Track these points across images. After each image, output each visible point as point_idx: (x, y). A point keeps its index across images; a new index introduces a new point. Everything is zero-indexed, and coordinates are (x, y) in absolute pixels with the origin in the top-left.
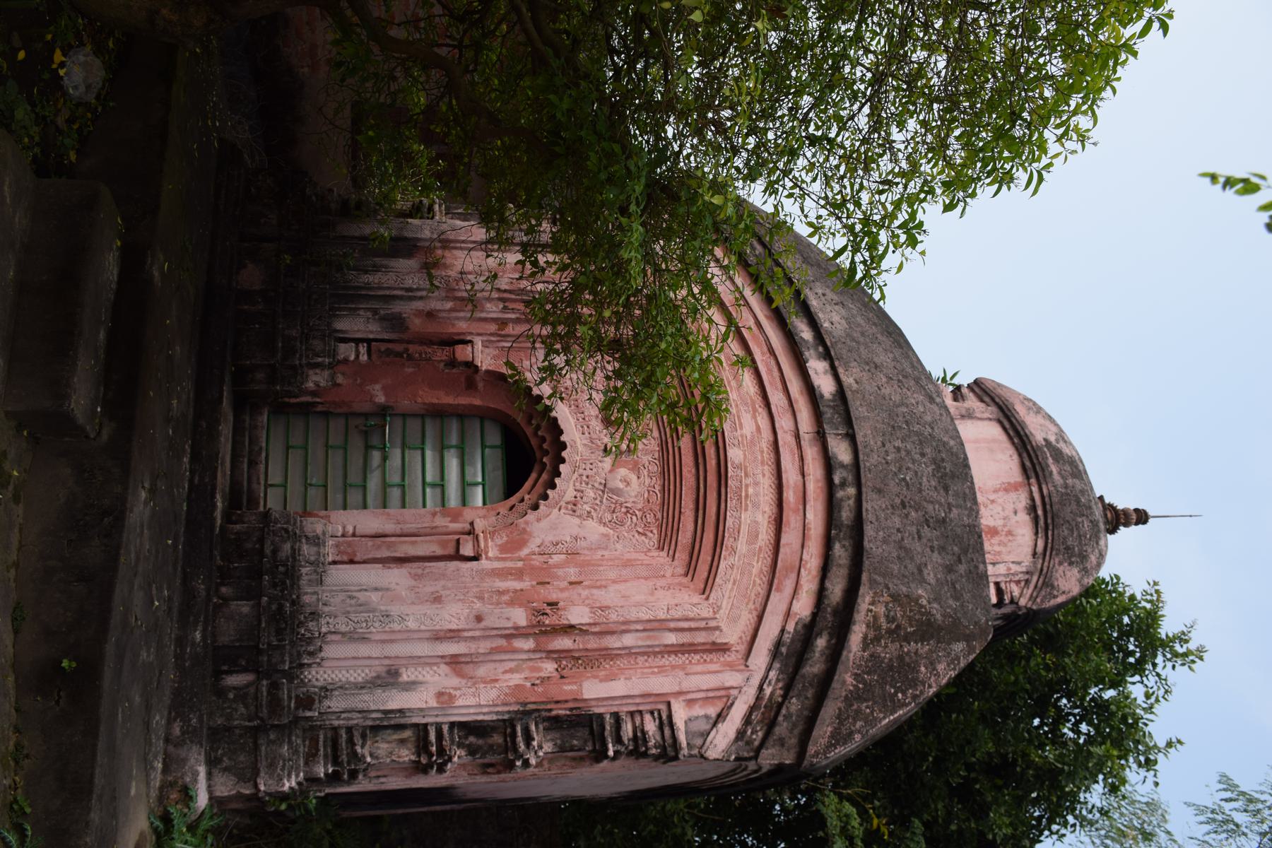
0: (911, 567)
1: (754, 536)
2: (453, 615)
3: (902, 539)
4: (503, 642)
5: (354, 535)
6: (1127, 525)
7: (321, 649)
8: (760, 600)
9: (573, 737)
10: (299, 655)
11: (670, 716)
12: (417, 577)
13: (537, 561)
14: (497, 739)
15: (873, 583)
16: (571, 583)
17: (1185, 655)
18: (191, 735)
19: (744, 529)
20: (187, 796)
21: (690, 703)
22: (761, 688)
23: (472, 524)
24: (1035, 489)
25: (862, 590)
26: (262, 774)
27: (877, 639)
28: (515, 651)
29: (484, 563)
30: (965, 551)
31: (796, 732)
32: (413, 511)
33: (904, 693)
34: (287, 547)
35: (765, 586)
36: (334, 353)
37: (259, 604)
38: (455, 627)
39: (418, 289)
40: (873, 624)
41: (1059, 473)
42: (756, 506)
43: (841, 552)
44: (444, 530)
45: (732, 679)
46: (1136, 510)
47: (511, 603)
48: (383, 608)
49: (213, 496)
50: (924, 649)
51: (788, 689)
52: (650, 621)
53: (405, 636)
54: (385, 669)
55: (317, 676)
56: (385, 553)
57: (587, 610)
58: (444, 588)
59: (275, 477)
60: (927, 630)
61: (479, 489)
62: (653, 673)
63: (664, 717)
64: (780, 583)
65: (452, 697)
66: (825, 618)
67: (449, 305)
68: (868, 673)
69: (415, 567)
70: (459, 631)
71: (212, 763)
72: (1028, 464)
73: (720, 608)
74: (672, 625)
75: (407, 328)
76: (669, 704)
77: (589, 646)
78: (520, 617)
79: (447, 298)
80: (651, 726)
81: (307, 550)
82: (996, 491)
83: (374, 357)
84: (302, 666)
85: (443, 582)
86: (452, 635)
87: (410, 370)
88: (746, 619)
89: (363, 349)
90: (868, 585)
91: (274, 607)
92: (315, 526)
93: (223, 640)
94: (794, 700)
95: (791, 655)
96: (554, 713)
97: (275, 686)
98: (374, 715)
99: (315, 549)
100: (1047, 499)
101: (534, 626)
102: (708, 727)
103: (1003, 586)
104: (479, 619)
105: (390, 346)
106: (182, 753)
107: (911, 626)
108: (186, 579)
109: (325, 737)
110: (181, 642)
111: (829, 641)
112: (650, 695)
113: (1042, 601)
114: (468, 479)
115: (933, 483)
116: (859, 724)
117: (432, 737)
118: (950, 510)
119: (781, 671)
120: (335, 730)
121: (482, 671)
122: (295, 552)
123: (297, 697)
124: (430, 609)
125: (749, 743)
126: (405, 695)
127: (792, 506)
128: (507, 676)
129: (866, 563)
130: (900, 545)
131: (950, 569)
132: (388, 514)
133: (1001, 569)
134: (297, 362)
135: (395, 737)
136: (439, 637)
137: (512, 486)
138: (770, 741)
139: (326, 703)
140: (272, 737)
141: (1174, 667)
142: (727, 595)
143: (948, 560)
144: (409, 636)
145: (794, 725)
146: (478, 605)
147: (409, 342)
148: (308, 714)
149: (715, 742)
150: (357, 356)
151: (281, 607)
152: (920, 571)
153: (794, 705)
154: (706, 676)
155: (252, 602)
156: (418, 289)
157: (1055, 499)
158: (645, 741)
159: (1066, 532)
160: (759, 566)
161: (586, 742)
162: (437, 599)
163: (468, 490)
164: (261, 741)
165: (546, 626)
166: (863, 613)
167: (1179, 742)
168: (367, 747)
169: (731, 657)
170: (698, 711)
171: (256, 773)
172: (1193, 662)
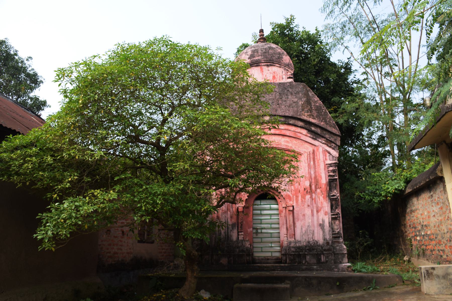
0: (294, 104)
2: (308, 212)
4: (313, 201)
5: (287, 235)
6: (263, 35)
8: (302, 141)
9: (333, 186)
10: (318, 245)
11: (329, 164)
12: (298, 220)
13: (293, 192)
14: (334, 202)
15: (300, 115)
17: (291, 19)
18: (336, 267)
19: (286, 144)
20: (349, 267)
21: (326, 159)
22: (323, 143)
24: (262, 64)
25: (302, 118)
27: (313, 116)
28: (315, 198)
29: (294, 205)
30: (286, 89)
31: (333, 136)
33: (323, 110)
34: (292, 249)
36: (242, 241)
40: (310, 116)
41: (258, 57)
42: (280, 140)
43: (292, 122)
45: (321, 150)
46: (260, 32)
47: (305, 199)
51: (323, 137)
55: (321, 241)
56: (292, 227)
57: (306, 182)
59: (269, 254)
60: (308, 102)
65: (326, 212)
67: (229, 213)
69: (296, 220)
71: (341, 263)
72: (255, 65)
78: (308, 197)
79: (227, 213)
80: (331, 169)
81: (292, 245)
82: (263, 75)
86: (312, 211)
88: (307, 145)
89: (240, 234)
92: (285, 244)
93: (315, 261)
95: (316, 136)
97: (325, 250)
104: (309, 206)
105: (239, 227)
106: (340, 268)
108: (303, 270)
110: (317, 270)
114: (269, 208)
117: (334, 216)
120: (333, 237)
121: (320, 205)
124: (306, 217)
125: (335, 147)
129: (295, 116)
130: (289, 107)
131: (292, 94)
133: (284, 77)
136: (313, 215)
139: (328, 239)
143: (289, 94)
144: (312, 221)
147: (238, 223)
151: (308, 249)
152: (294, 102)
153: (327, 136)
154: (320, 156)
157: (266, 59)
158: (334, 170)
160: (294, 141)
162: (304, 215)
165: (310, 191)
169: (315, 150)
170: (328, 158)
171: (343, 254)
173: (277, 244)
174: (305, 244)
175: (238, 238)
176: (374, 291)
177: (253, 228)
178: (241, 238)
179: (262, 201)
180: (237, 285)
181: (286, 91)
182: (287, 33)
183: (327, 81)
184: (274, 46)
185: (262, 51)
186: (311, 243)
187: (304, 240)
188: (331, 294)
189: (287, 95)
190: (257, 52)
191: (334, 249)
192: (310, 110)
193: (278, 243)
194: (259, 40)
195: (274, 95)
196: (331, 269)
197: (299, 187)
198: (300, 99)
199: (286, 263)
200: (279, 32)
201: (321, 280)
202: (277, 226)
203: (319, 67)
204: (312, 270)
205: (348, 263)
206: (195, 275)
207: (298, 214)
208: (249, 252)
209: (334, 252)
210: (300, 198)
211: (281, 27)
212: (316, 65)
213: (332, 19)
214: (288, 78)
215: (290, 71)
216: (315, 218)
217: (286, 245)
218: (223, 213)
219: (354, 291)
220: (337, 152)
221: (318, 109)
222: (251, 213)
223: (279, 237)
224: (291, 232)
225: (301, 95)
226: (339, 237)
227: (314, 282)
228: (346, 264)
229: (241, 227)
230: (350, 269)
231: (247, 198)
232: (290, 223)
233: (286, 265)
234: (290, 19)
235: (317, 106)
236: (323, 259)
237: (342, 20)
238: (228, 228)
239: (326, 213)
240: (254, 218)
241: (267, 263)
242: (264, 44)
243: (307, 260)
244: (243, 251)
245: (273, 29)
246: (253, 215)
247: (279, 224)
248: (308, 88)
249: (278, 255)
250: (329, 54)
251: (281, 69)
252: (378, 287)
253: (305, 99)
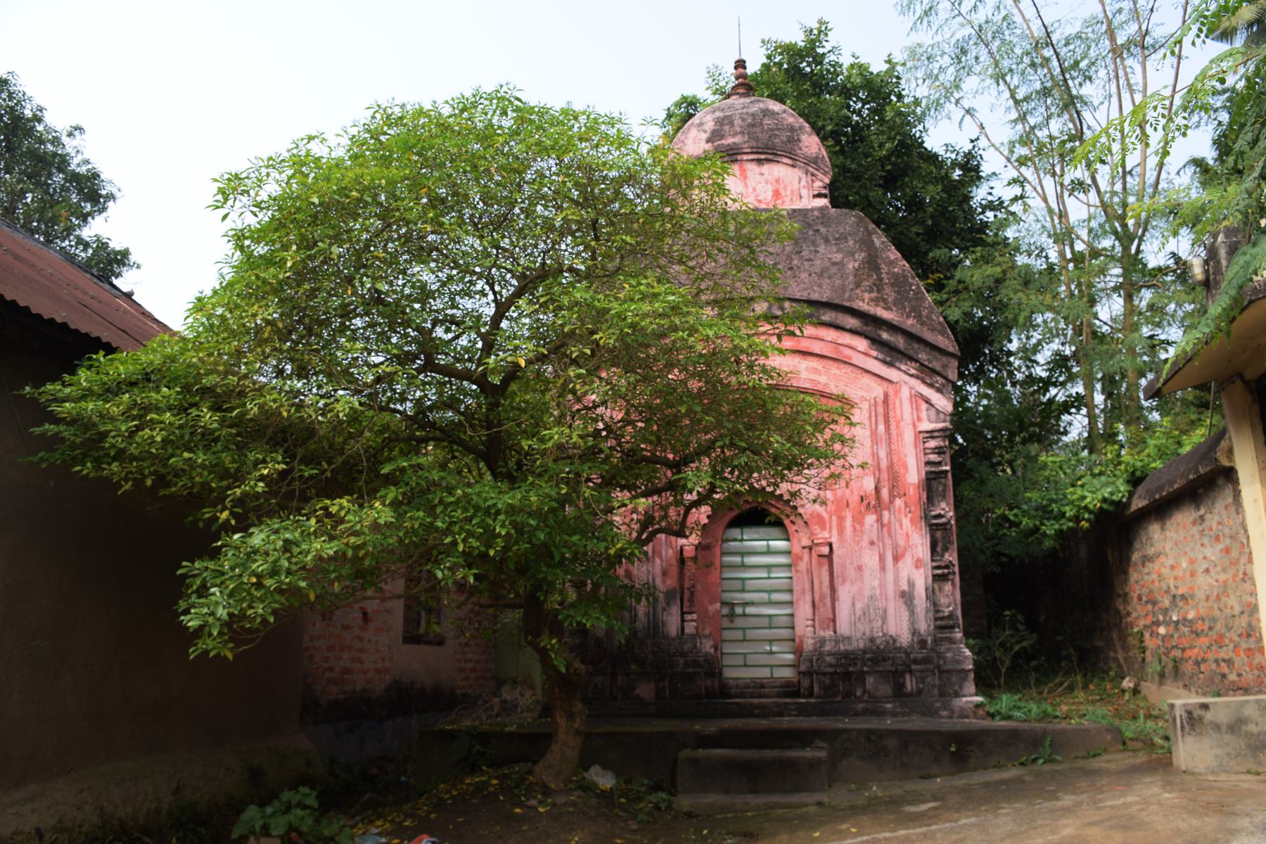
0: (834, 270)
1: (816, 371)
2: (870, 559)
4: (885, 529)
5: (813, 620)
8: (855, 370)
12: (844, 581)
13: (831, 507)
14: (939, 534)
15: (850, 299)
17: (820, 32)
18: (946, 706)
19: (812, 376)
20: (978, 706)
21: (919, 419)
22: (911, 376)
24: (745, 157)
28: (889, 522)
29: (834, 540)
30: (810, 226)
34: (828, 659)
36: (693, 637)
40: (876, 301)
41: (733, 136)
43: (827, 316)
45: (905, 393)
46: (736, 68)
47: (862, 524)
50: (884, 269)
51: (912, 359)
55: (905, 638)
56: (828, 601)
59: (765, 673)
60: (872, 263)
65: (918, 560)
67: (658, 561)
69: (837, 582)
78: (870, 519)
79: (653, 562)
80: (932, 444)
82: (746, 186)
86: (882, 558)
88: (867, 380)
89: (688, 617)
92: (809, 644)
93: (889, 691)
95: (892, 355)
97: (915, 661)
104: (872, 543)
105: (686, 600)
106: (957, 709)
108: (857, 714)
114: (765, 550)
117: (939, 572)
120: (937, 627)
121: (901, 542)
122: (830, 654)
124: (867, 572)
129: (836, 301)
130: (821, 275)
131: (827, 241)
133: (804, 192)
136: (883, 568)
143: (820, 241)
144: (882, 585)
147: (682, 588)
151: (869, 659)
152: (835, 264)
153: (923, 356)
154: (904, 409)
157: (754, 144)
158: (941, 447)
160: (834, 369)
162: (860, 568)
165: (875, 503)
169: (891, 393)
170: (924, 414)
171: (963, 671)
173: (787, 646)
174: (861, 645)
175: (683, 629)
176: (1048, 767)
177: (724, 603)
178: (690, 628)
179: (746, 530)
180: (685, 753)
181: (811, 233)
182: (808, 69)
183: (914, 204)
184: (775, 106)
185: (743, 120)
186: (878, 642)
187: (859, 635)
188: (936, 776)
189: (813, 243)
190: (731, 124)
191: (938, 657)
192: (878, 286)
193: (790, 643)
194: (733, 88)
196: (931, 712)
197: (848, 492)
198: (851, 254)
199: (811, 695)
200: (785, 66)
201: (907, 738)
202: (785, 597)
203: (893, 164)
204: (880, 713)
206: (576, 725)
207: (843, 565)
208: (712, 667)
209: (938, 667)
210: (848, 522)
211: (790, 51)
212: (887, 158)
213: (931, 33)
215: (820, 176)
216: (890, 576)
217: (811, 648)
219: (995, 767)
220: (949, 399)
221: (899, 283)
223: (793, 628)
224: (825, 611)
225: (851, 243)
226: (952, 627)
227: (892, 743)
228: (971, 698)
229: (691, 600)
230: (981, 712)
231: (706, 521)
232: (821, 589)
233: (813, 700)
234: (815, 32)
236: (910, 684)
237: (959, 36)
238: (656, 600)
239: (918, 564)
240: (725, 576)
241: (761, 696)
242: (747, 100)
243: (868, 687)
244: (695, 663)
245: (769, 57)
246: (722, 567)
247: (791, 591)
248: (872, 226)
249: (788, 673)
250: (920, 127)
251: (796, 170)
252: (1058, 758)
253: (863, 255)
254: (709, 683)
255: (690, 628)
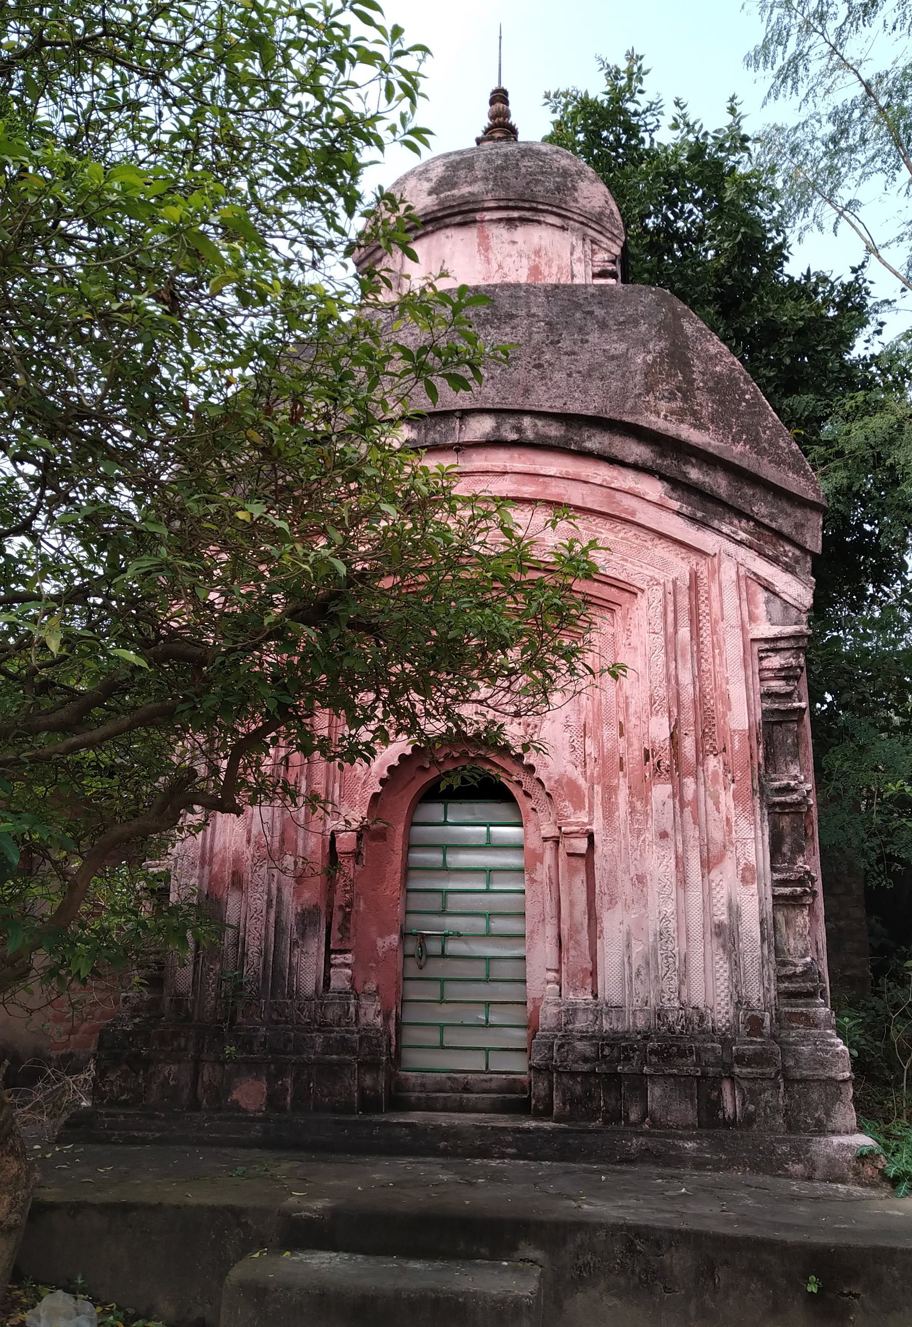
0: (611, 366)
2: (659, 864)
3: (579, 372)
4: (688, 810)
5: (558, 971)
6: (507, 114)
7: (696, 1008)
8: (642, 534)
9: (783, 743)
10: (703, 1032)
11: (766, 640)
12: (613, 902)
13: (593, 769)
14: (785, 822)
15: (634, 411)
16: (621, 734)
17: (630, 75)
18: (800, 1153)
20: (864, 1157)
21: (752, 618)
22: (740, 543)
23: (545, 839)
24: (488, 216)
26: (833, 1074)
27: (694, 413)
30: (578, 306)
32: (528, 905)
33: (744, 392)
34: (580, 1046)
35: (627, 527)
37: (651, 1076)
38: (673, 861)
39: (269, 893)
40: (680, 415)
41: (470, 184)
43: (596, 442)
44: (553, 870)
45: (728, 572)
46: (492, 102)
47: (646, 801)
48: (651, 940)
49: (528, 1131)
50: (698, 366)
52: (666, 653)
53: (682, 916)
54: (715, 940)
55: (722, 1013)
56: (584, 936)
57: (654, 719)
58: (627, 871)
59: (475, 1062)
60: (678, 357)
61: (492, 828)
62: (720, 654)
63: (767, 646)
64: (625, 511)
65: (747, 868)
66: (668, 467)
68: (731, 428)
70: (677, 857)
71: (821, 1129)
72: (458, 219)
73: (652, 578)
74: (671, 630)
75: (315, 906)
76: (753, 640)
77: (692, 720)
78: (661, 791)
80: (776, 661)
81: (581, 1023)
83: (348, 946)
84: (714, 1030)
85: (619, 873)
86: (681, 863)
87: (362, 903)
88: (662, 550)
89: (338, 959)
90: (637, 417)
91: (654, 1059)
92: (548, 1015)
93: (691, 1116)
94: (755, 509)
95: (705, 506)
96: (761, 761)
97: (740, 1059)
98: (766, 952)
99: (580, 1014)
100: (502, 204)
101: (672, 777)
102: (778, 601)
103: (597, 270)
104: (664, 835)
105: (335, 926)
106: (821, 1162)
107: (676, 375)
108: (628, 1160)
109: (787, 1005)
110: (700, 1165)
111: (693, 466)
112: (745, 659)
113: (617, 228)
115: (508, 330)
116: (782, 444)
117: (787, 890)
118: (534, 315)
119: (721, 520)
120: (780, 993)
121: (717, 835)
123: (749, 1034)
124: (653, 889)
126: (745, 917)
127: (540, 489)
128: (723, 808)
129: (611, 415)
130: (588, 375)
131: (603, 326)
132: (532, 932)
133: (579, 268)
134: (357, 1036)
135: (784, 930)
136: (683, 881)
137: (493, 792)
138: (798, 538)
139: (754, 1003)
140: (792, 1063)
141: (641, 92)
142: (641, 570)
143: (591, 325)
145: (782, 511)
146: (649, 836)
147: (330, 905)
148: (767, 1022)
149: (795, 596)
150: (347, 965)
151: (653, 1052)
152: (613, 358)
154: (726, 600)
155: (615, 1084)
156: (269, 893)
159: (539, 188)
161: (789, 730)
162: (641, 879)
163: (495, 842)
164: (798, 1075)
166: (669, 425)
167: (732, 99)
168: (796, 961)
169: (703, 571)
170: (761, 610)
171: (832, 1080)
172: (640, 68)
174: (641, 1023)
175: (327, 980)
178: (340, 979)
179: (452, 807)
189: (581, 329)
192: (686, 392)
193: (516, 1010)
195: (521, 331)
196: (771, 1165)
199: (546, 1113)
205: (861, 1129)
207: (612, 873)
213: (796, 100)
214: (595, 276)
215: (606, 243)
216: (695, 896)
217: (552, 1022)
218: (262, 858)
220: (805, 583)
221: (722, 388)
222: (397, 860)
224: (577, 957)
226: (811, 995)
227: (678, 1261)
230: (869, 1171)
231: (378, 789)
232: (571, 915)
233: (548, 1125)
235: (719, 378)
236: (731, 1102)
239: (747, 875)
240: (412, 885)
241: (462, 1108)
244: (344, 1045)
246: (407, 869)
248: (681, 307)
249: (517, 1064)
253: (662, 344)
254: (368, 1081)
255: (340, 979)
